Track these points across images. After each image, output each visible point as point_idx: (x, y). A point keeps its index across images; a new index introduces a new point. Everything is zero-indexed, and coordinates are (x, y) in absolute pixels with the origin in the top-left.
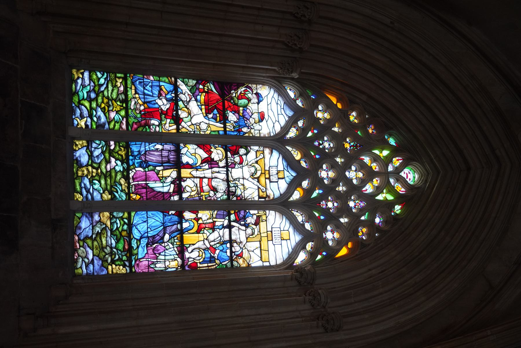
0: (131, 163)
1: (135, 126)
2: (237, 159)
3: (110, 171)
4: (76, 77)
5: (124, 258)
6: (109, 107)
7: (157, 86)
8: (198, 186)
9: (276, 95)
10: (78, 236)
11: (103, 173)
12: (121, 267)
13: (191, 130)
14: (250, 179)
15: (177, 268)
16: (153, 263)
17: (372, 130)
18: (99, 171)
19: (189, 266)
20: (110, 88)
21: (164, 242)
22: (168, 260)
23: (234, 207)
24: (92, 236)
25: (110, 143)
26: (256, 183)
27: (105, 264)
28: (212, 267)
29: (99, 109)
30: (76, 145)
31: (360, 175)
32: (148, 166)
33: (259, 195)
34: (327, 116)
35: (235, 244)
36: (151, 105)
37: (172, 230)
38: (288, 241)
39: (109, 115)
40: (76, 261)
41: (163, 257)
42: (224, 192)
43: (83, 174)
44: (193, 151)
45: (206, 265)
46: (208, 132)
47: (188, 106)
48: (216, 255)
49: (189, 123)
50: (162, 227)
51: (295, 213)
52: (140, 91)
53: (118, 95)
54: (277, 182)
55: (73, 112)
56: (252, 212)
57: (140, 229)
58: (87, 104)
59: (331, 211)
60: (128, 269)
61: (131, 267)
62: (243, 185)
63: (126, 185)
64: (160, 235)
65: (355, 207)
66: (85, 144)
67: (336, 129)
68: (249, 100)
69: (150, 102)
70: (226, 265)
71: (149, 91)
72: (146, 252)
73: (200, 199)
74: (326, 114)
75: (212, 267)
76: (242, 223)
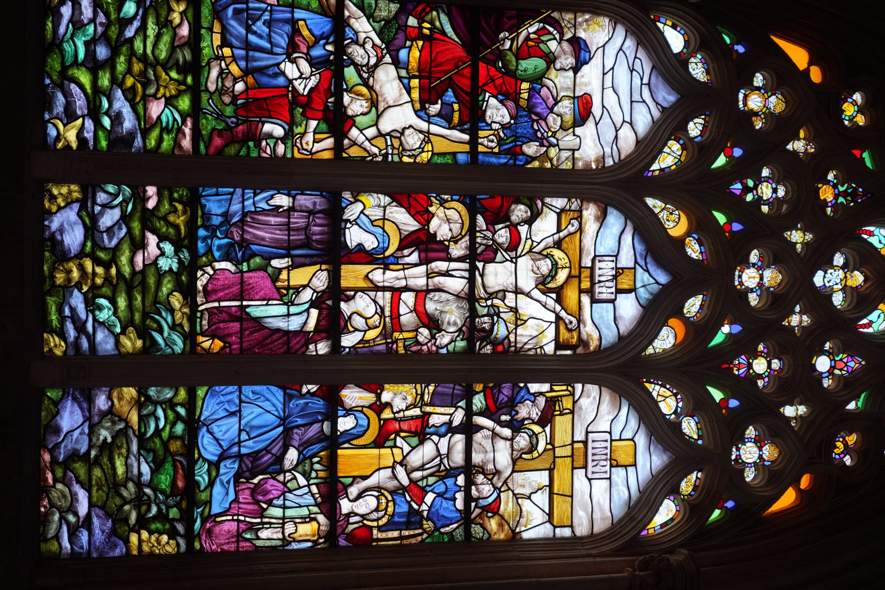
1: (218, 141)
2: (503, 235)
3: (143, 272)
5: (174, 513)
6: (145, 86)
7: (285, 21)
8: (387, 313)
9: (630, 44)
10: (51, 451)
11: (124, 276)
12: (165, 538)
13: (376, 150)
14: (536, 294)
15: (315, 543)
16: (251, 527)
18: (113, 271)
19: (350, 537)
20: (152, 30)
21: (283, 471)
22: (292, 519)
23: (486, 372)
25: (145, 191)
26: (551, 303)
28: (413, 541)
29: (119, 93)
30: (53, 198)
31: (857, 279)
32: (247, 258)
34: (776, 103)
35: (480, 478)
36: (265, 80)
38: (629, 469)
39: (145, 109)
40: (45, 520)
41: (277, 512)
42: (460, 330)
43: (69, 280)
44: (376, 214)
45: (396, 534)
46: (425, 157)
48: (424, 507)
49: (371, 132)
50: (281, 429)
51: (655, 390)
52: (236, 38)
53: (173, 49)
55: (49, 105)
56: (534, 387)
57: (218, 435)
58: (85, 78)
59: (760, 383)
60: (182, 542)
61: (190, 536)
62: (515, 310)
63: (186, 310)
64: (274, 451)
65: (831, 372)
67: (798, 146)
68: (550, 59)
69: (262, 70)
70: (450, 534)
71: (260, 37)
72: (232, 496)
73: (389, 350)
74: (773, 99)
75: (413, 541)
76: (504, 418)
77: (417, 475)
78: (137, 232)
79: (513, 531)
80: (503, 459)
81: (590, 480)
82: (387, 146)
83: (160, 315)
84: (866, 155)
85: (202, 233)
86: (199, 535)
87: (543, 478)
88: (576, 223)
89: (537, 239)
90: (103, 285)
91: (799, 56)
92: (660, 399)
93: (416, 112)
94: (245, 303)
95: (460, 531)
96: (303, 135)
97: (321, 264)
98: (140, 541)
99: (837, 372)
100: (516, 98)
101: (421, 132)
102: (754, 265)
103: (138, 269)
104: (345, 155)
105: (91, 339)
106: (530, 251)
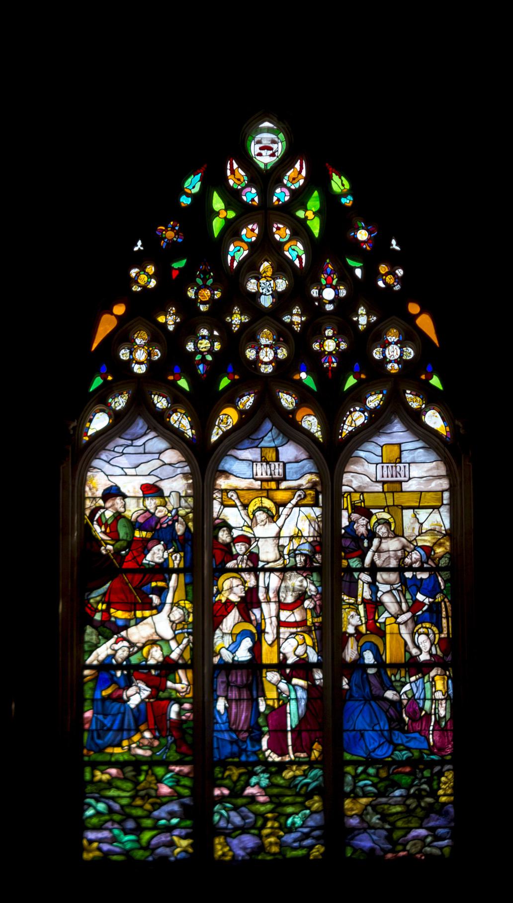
0: (253, 758)
1: (184, 749)
2: (240, 548)
3: (270, 796)
4: (97, 853)
5: (427, 773)
6: (150, 797)
8: (294, 630)
9: (104, 456)
12: (443, 779)
13: (185, 641)
14: (280, 522)
15: (449, 677)
16: (437, 722)
17: (166, 230)
18: (270, 815)
20: (112, 793)
21: (401, 700)
22: (433, 694)
23: (334, 557)
24: (387, 830)
25: (218, 796)
27: (437, 807)
29: (156, 813)
30: (224, 854)
32: (259, 728)
33: (311, 506)
35: (408, 560)
36: (142, 718)
37: (379, 685)
38: (404, 447)
39: (165, 796)
40: (429, 856)
41: (428, 704)
42: (306, 578)
43: (276, 844)
44: (228, 640)
46: (188, 605)
47: (139, 645)
48: (427, 601)
49: (173, 644)
50: (373, 703)
51: (347, 428)
52: (115, 738)
53: (126, 779)
54: (285, 464)
55: (165, 858)
56: (345, 522)
57: (376, 744)
58: (146, 836)
60: (447, 767)
61: (442, 762)
62: (291, 538)
63: (294, 768)
65: (335, 288)
66: (222, 840)
68: (118, 516)
70: (445, 582)
71: (114, 721)
72: (417, 735)
74: (138, 341)
75: (449, 608)
76: (366, 544)
77: (404, 606)
78: (244, 801)
79: (445, 535)
80: (393, 545)
81: (410, 479)
82: (183, 633)
83: (297, 785)
84: (176, 265)
85: (243, 758)
86: (442, 756)
87: (408, 514)
88: (230, 494)
89: (242, 523)
90: (278, 821)
91: (106, 326)
92: (353, 425)
93: (159, 612)
94: (289, 729)
95: (443, 573)
96: (177, 691)
97: (262, 677)
98: (444, 795)
99: (334, 282)
100: (144, 541)
101: (172, 609)
102: (258, 353)
103: (268, 800)
104: (189, 662)
105: (314, 829)
106: (250, 527)
